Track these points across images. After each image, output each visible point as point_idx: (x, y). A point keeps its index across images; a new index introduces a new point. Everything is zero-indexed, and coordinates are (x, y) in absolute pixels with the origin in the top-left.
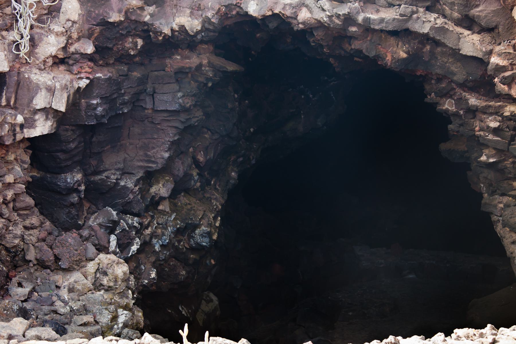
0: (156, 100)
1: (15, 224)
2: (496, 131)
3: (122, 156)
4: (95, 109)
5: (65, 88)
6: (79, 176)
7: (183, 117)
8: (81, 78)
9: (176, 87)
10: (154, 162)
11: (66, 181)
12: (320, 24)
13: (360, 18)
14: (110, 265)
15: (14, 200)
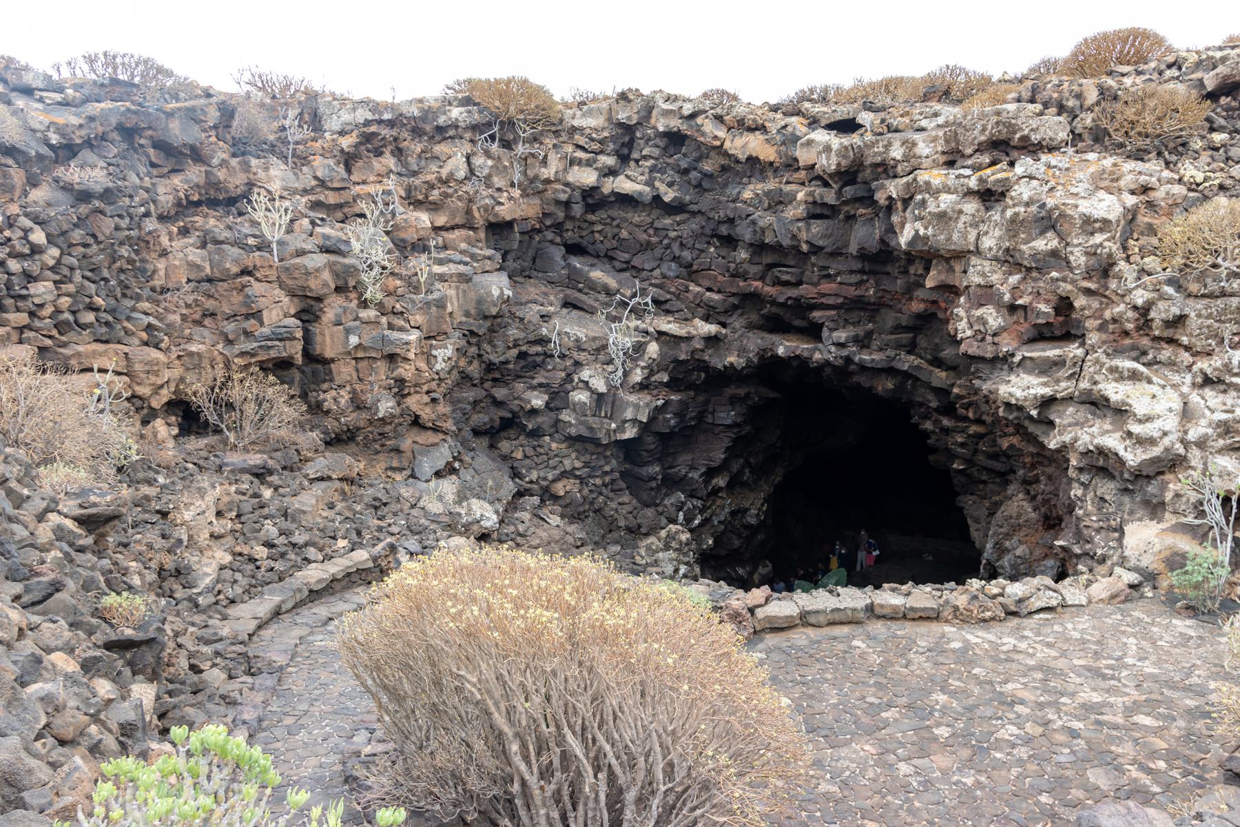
1: (612, 500)
2: (962, 445)
3: (690, 457)
5: (647, 405)
7: (736, 430)
9: (730, 408)
12: (827, 363)
13: (856, 359)
14: (677, 532)
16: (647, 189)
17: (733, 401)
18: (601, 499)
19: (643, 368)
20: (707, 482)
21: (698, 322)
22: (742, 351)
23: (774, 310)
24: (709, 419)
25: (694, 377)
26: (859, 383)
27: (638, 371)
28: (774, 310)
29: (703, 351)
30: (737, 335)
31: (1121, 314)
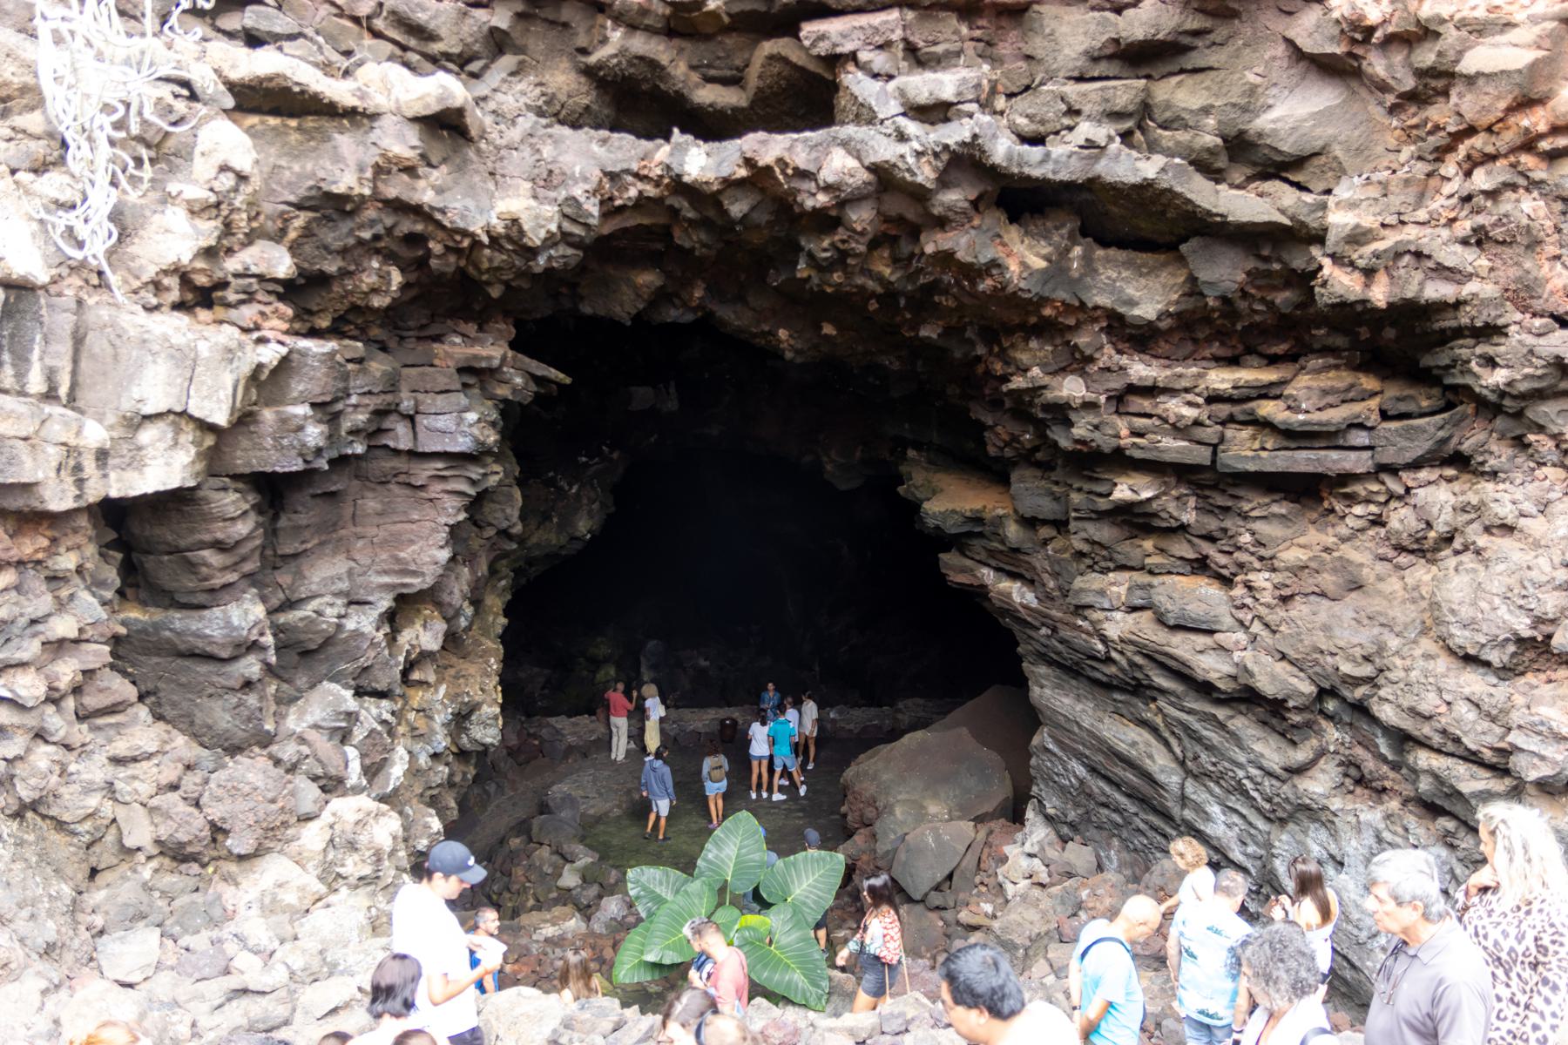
0: (419, 428)
1: (83, 751)
2: (1179, 429)
4: (301, 428)
5: (229, 355)
6: (258, 611)
7: (475, 472)
8: (262, 341)
9: (463, 400)
10: (414, 573)
11: (228, 623)
15: (77, 690)
17: (475, 375)
18: (43, 756)
19: (197, 211)
20: (392, 639)
21: (397, 71)
22: (546, 180)
23: (640, 44)
24: (401, 437)
25: (368, 280)
26: (946, 258)
27: (176, 217)
28: (640, 44)
29: (410, 170)
30: (515, 134)
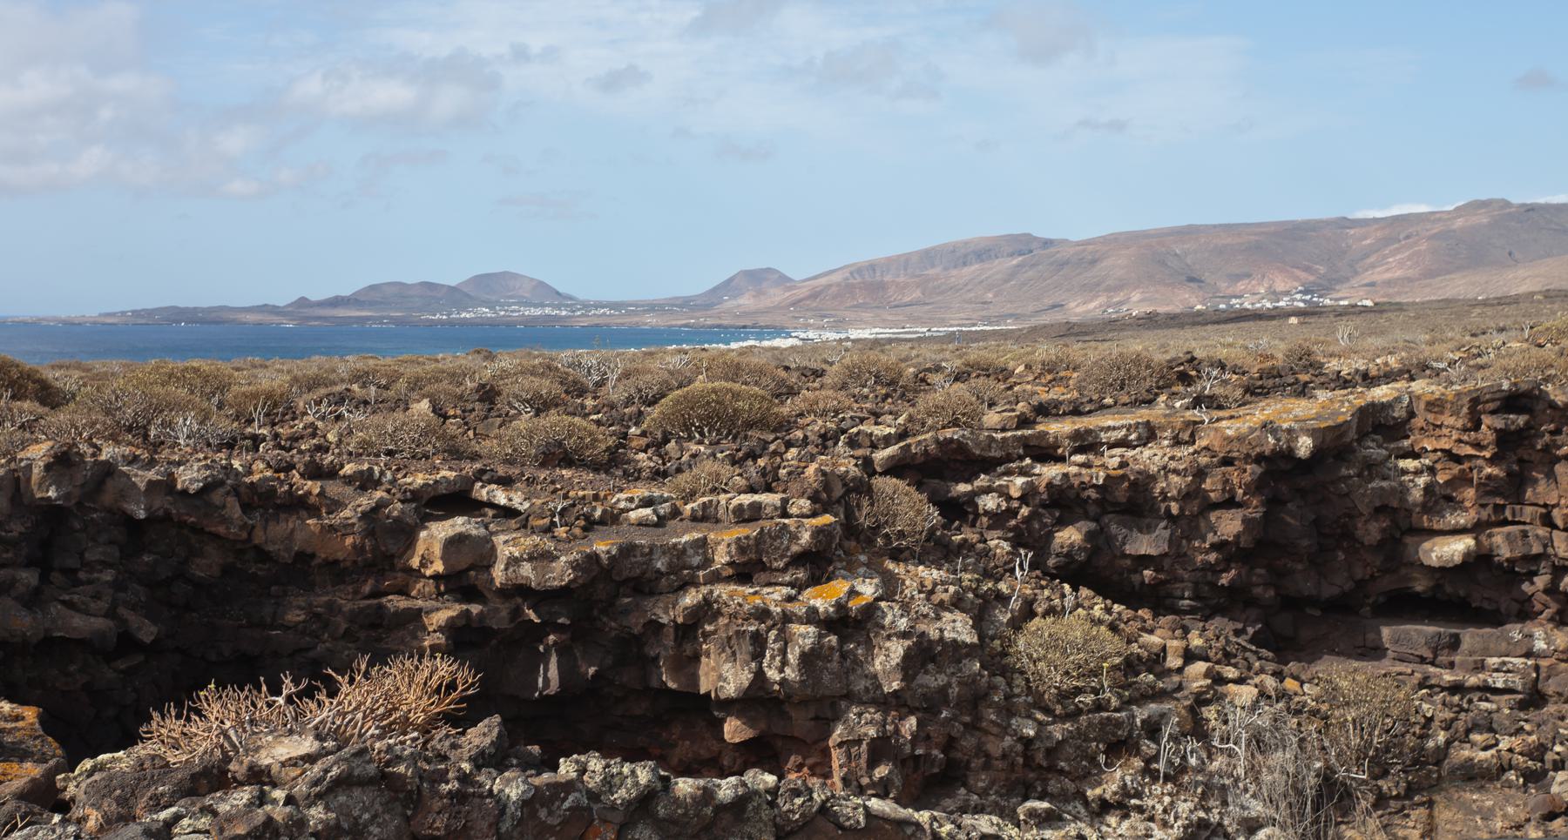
16: (110, 623)
31: (1011, 748)
